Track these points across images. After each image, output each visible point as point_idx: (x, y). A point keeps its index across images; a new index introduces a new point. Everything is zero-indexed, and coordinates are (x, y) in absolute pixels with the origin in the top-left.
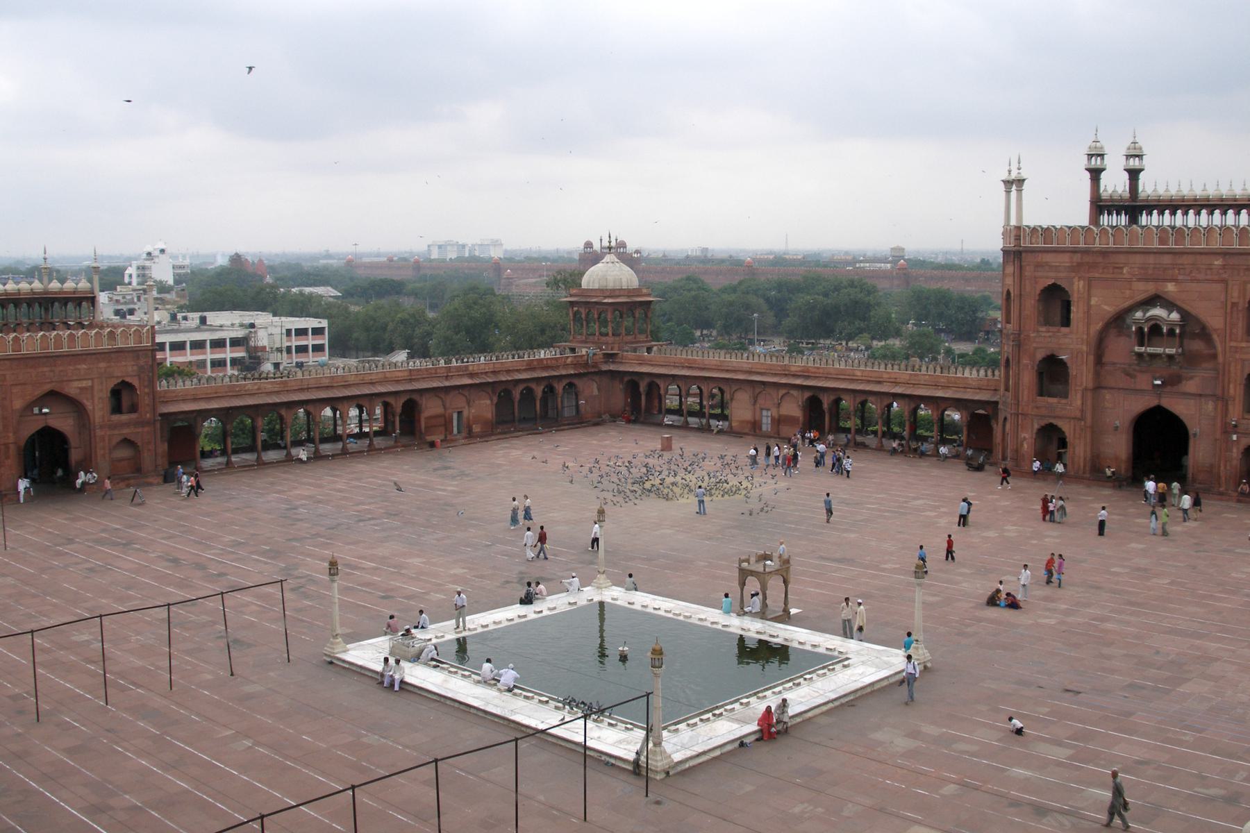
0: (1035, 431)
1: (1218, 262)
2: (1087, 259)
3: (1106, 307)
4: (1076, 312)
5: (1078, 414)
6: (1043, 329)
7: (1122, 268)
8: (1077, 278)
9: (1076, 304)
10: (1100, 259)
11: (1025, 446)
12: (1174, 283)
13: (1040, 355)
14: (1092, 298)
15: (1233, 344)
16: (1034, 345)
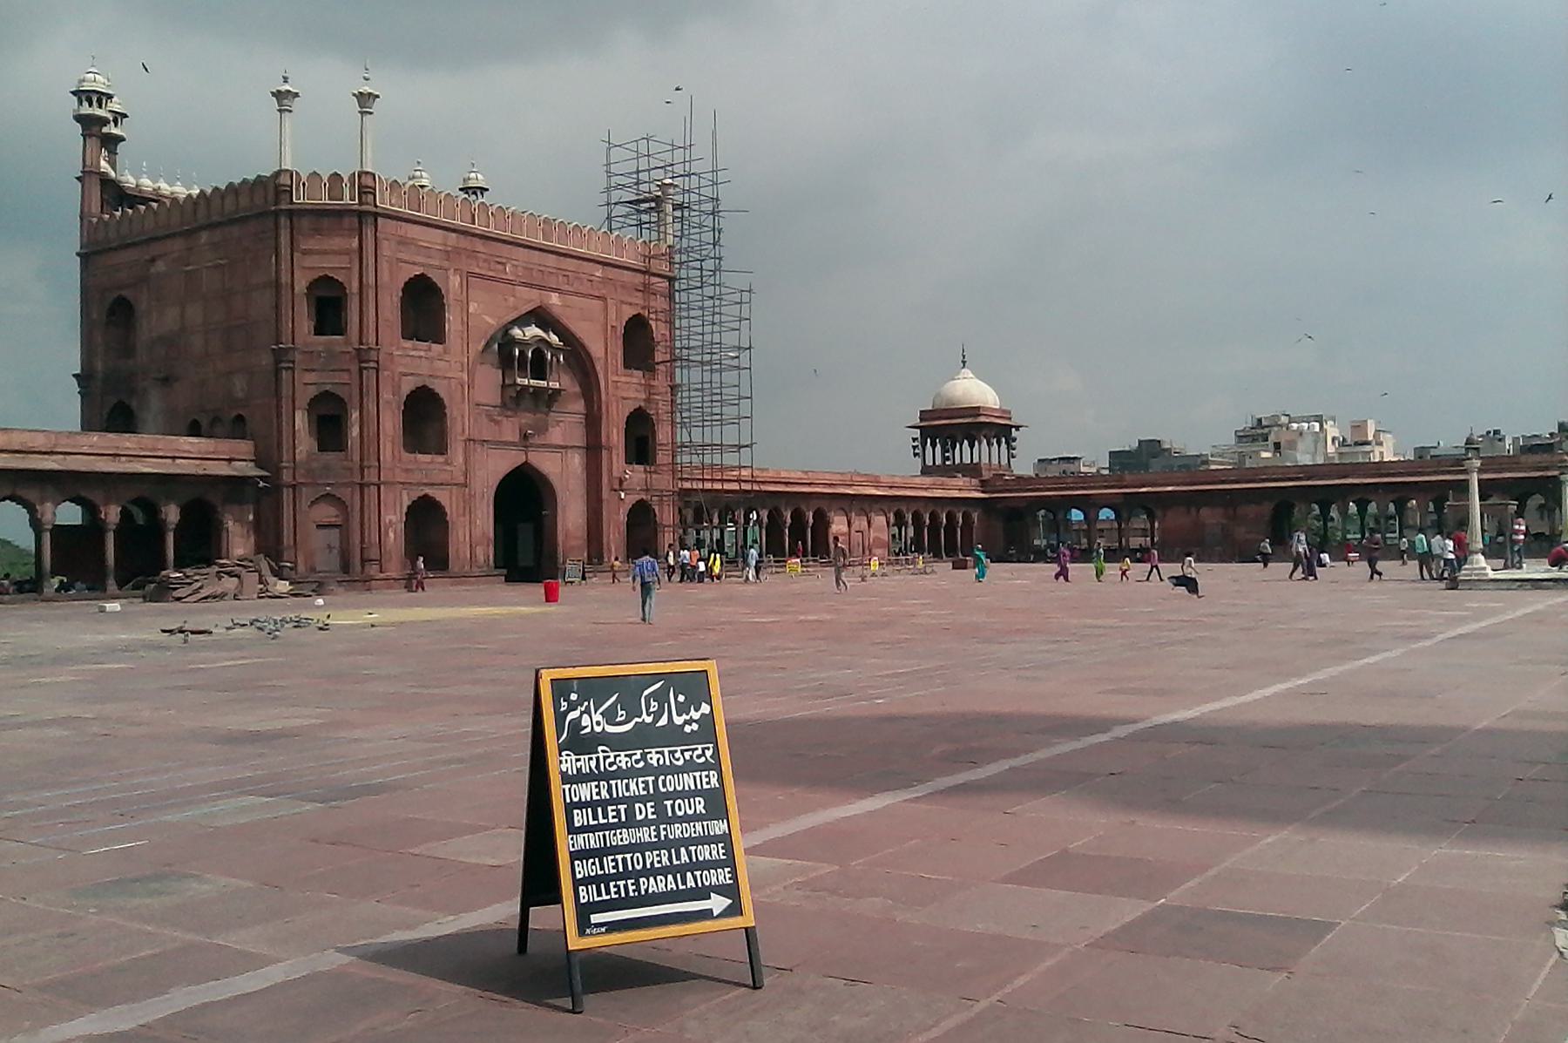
0: (405, 510)
1: (599, 272)
2: (465, 242)
3: (488, 319)
4: (452, 321)
5: (461, 480)
6: (408, 344)
7: (504, 264)
8: (452, 270)
9: (452, 309)
10: (479, 245)
11: (391, 535)
12: (557, 294)
13: (408, 386)
14: (471, 304)
15: (616, 378)
16: (401, 369)
